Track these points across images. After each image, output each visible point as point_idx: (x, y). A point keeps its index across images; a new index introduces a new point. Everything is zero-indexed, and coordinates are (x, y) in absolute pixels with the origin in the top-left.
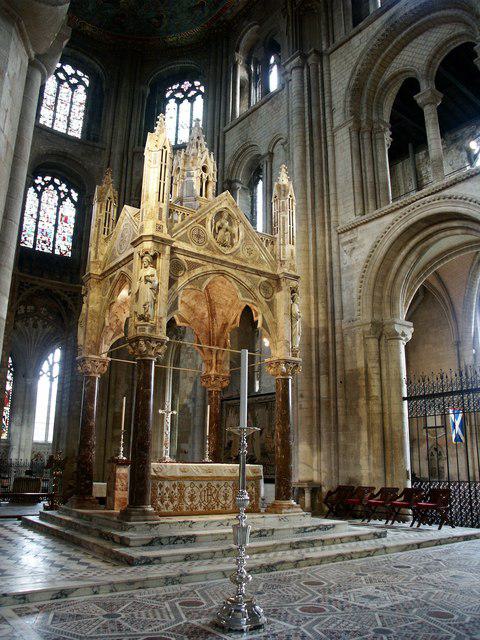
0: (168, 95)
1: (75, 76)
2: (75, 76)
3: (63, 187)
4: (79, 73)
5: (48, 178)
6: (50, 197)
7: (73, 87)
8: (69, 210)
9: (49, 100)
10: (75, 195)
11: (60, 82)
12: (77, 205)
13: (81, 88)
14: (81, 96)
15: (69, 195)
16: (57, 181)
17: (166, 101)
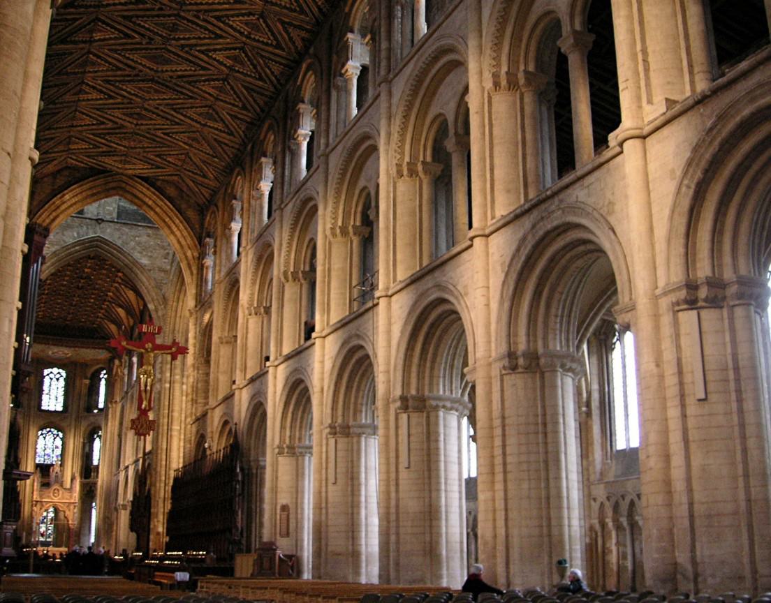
0: (101, 376)
1: (59, 373)
2: (59, 373)
3: (55, 432)
4: (61, 371)
5: (48, 429)
6: (50, 438)
7: (58, 379)
8: (59, 442)
9: (46, 387)
10: (61, 435)
11: (51, 379)
12: (62, 439)
13: (62, 380)
14: (62, 383)
15: (58, 435)
16: (52, 430)
17: (100, 379)
